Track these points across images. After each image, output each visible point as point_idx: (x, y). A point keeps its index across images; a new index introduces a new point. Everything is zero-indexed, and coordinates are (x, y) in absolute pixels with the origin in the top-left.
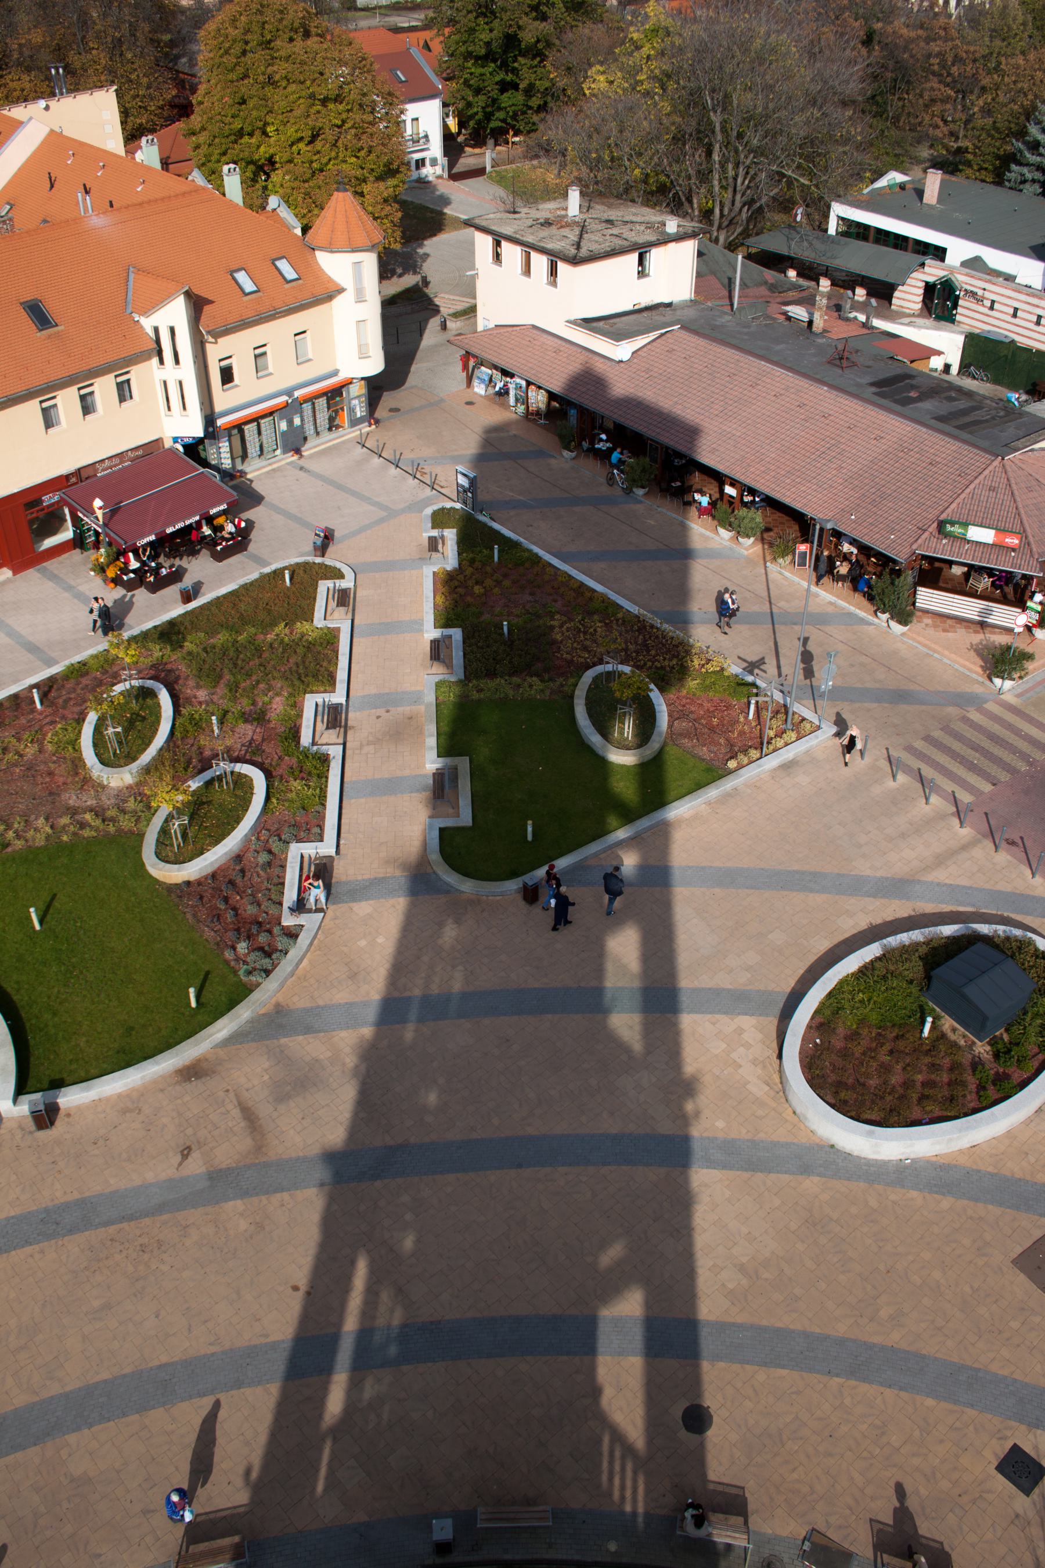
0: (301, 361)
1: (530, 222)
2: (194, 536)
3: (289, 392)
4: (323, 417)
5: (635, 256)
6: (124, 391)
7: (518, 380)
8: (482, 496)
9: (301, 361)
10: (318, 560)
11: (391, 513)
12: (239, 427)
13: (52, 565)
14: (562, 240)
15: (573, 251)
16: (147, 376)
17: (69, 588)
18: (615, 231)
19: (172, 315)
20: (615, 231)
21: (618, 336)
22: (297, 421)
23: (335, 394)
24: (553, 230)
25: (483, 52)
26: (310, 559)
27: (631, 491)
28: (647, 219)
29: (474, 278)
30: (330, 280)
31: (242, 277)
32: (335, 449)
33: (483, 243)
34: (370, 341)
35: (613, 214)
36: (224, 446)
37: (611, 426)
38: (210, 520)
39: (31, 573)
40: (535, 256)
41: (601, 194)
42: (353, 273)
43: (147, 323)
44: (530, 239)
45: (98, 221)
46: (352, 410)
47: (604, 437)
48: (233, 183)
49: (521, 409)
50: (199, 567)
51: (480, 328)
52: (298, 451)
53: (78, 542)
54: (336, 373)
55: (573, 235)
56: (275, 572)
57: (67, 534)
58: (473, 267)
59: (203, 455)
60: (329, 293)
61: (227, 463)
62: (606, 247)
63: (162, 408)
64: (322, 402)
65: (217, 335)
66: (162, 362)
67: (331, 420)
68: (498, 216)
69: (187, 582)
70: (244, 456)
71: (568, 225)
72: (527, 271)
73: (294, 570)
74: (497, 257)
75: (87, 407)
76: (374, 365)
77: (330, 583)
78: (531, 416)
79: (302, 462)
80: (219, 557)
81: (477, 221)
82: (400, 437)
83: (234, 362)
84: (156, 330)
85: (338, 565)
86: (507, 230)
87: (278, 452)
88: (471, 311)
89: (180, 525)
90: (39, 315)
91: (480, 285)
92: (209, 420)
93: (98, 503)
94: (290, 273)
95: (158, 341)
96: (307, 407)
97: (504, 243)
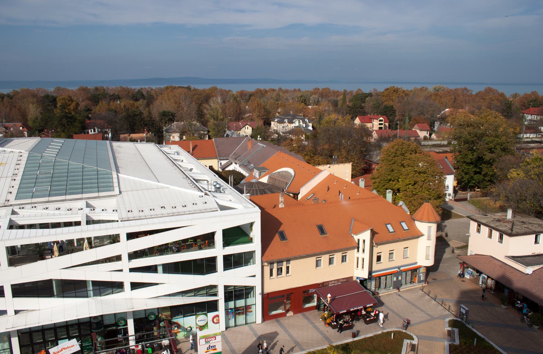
0: (405, 257)
1: (492, 219)
2: (359, 313)
3: (399, 268)
4: (409, 278)
5: (534, 236)
6: (344, 259)
7: (484, 275)
8: (470, 318)
9: (405, 257)
10: (404, 331)
11: (432, 318)
12: (379, 277)
13: (307, 313)
14: (506, 227)
15: (510, 231)
16: (352, 255)
17: (312, 323)
18: (526, 226)
19: (366, 236)
20: (526, 226)
21: (527, 264)
22: (400, 278)
23: (414, 271)
24: (501, 223)
25: (470, 161)
26: (401, 330)
27: (532, 326)
28: (538, 223)
29: (469, 236)
30: (419, 231)
31: (389, 226)
32: (412, 290)
33: (473, 225)
34: (430, 254)
35: (524, 220)
36: (373, 283)
37: (521, 298)
38: (365, 308)
39: (299, 315)
40: (493, 231)
41: (519, 212)
42: (427, 230)
43: (356, 237)
44: (493, 225)
45: (345, 203)
46: (419, 277)
47: (519, 302)
48: (389, 196)
49: (484, 286)
50: (359, 325)
51: (469, 254)
52: (398, 289)
53: (318, 307)
54: (416, 263)
55: (509, 226)
56: (388, 332)
57: (315, 304)
58: (469, 233)
59: (365, 284)
60: (419, 235)
61: (373, 289)
62: (523, 231)
63: (355, 267)
64: (409, 273)
65: (378, 244)
66: (358, 251)
67: (411, 279)
68: (480, 216)
69: (354, 330)
70: (379, 287)
71: (507, 222)
72: (490, 236)
73: (395, 333)
74: (479, 231)
75: (331, 262)
76: (430, 262)
77: (409, 341)
78: (486, 289)
79: (399, 293)
80: (367, 323)
81: (472, 217)
82: (436, 290)
83: (382, 255)
84: (359, 240)
85: (412, 334)
86: (484, 221)
87: (391, 288)
88: (466, 247)
89: (356, 309)
90: (321, 230)
91: (470, 238)
92: (370, 273)
93: (329, 295)
94: (405, 227)
95: (358, 244)
96: (404, 273)
97: (482, 226)
